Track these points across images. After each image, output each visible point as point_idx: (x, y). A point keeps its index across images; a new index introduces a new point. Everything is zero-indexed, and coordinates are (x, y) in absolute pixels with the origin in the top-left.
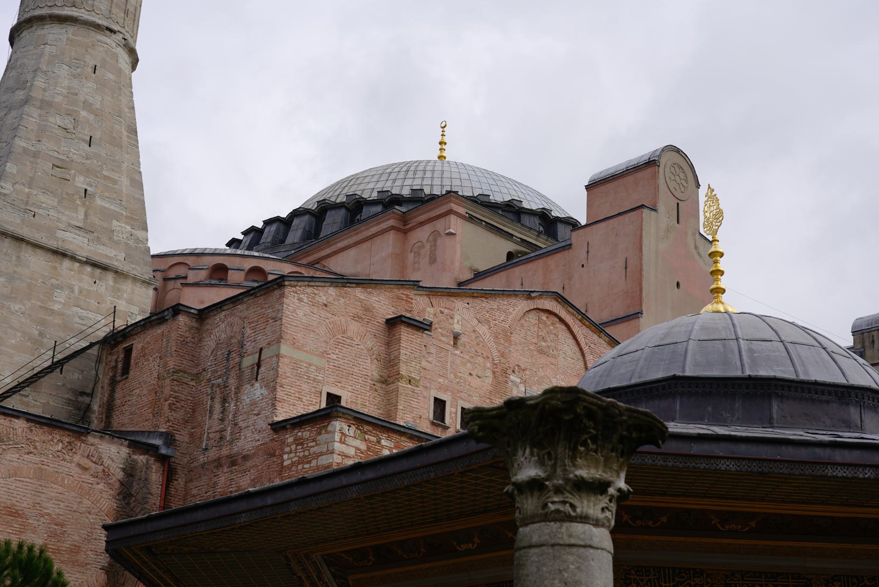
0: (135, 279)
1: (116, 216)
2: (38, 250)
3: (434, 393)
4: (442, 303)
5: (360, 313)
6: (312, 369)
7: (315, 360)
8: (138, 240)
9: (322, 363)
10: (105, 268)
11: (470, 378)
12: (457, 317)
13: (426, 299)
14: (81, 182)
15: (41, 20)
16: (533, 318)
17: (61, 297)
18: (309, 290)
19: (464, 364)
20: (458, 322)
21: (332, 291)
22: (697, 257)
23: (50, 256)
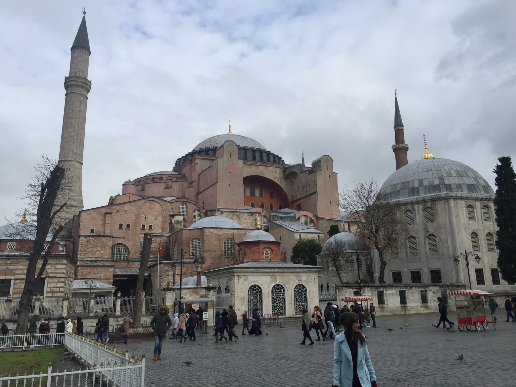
0: (79, 207)
1: (75, 196)
3: (119, 223)
4: (122, 206)
7: (88, 224)
8: (80, 199)
11: (129, 218)
12: (126, 207)
13: (117, 206)
16: (148, 202)
19: (128, 216)
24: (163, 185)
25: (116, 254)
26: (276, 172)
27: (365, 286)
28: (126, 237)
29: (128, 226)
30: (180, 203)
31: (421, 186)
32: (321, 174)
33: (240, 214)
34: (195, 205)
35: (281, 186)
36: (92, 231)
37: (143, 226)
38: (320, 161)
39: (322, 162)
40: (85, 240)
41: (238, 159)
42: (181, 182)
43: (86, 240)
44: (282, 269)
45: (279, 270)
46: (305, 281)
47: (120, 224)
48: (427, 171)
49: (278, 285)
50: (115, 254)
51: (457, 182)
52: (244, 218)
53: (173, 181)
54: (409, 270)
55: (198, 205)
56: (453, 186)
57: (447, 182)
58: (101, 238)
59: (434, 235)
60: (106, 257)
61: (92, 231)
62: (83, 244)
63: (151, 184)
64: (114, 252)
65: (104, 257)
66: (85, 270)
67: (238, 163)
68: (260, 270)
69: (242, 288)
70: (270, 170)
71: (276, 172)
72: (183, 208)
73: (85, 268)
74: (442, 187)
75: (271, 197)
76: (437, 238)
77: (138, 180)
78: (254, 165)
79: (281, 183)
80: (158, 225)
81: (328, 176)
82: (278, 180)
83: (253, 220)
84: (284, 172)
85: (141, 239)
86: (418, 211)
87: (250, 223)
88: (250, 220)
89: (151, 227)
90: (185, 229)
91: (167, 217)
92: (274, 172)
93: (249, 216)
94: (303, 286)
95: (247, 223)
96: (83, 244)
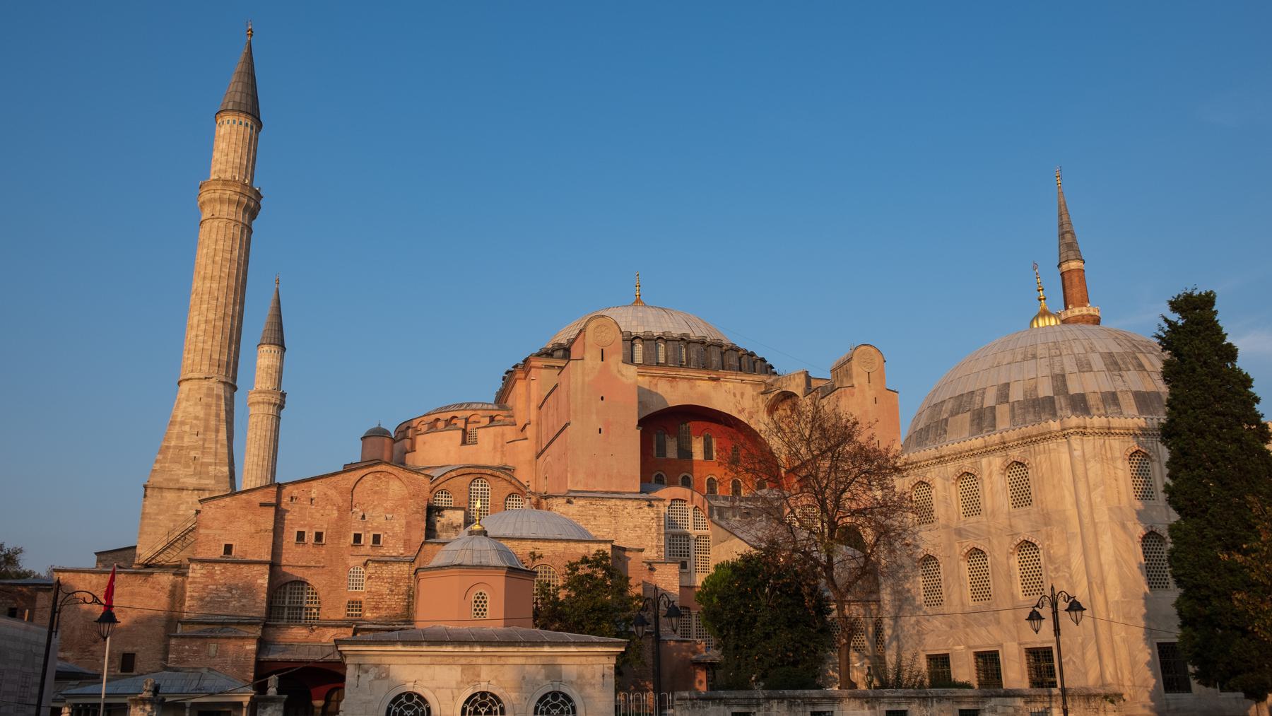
2: (170, 491)
5: (244, 505)
6: (217, 536)
7: (219, 532)
8: (222, 472)
9: (223, 531)
10: (203, 490)
12: (314, 490)
14: (193, 454)
15: (181, 381)
16: (370, 477)
17: (183, 507)
18: (215, 502)
19: (318, 511)
20: (314, 493)
21: (228, 499)
22: (620, 377)
23: (176, 491)
24: (458, 435)
25: (289, 608)
26: (742, 394)
27: (768, 699)
28: (313, 564)
29: (319, 536)
31: (1002, 403)
32: (853, 395)
36: (228, 549)
37: (357, 538)
38: (849, 360)
39: (854, 362)
40: (202, 571)
41: (623, 362)
42: (498, 428)
43: (204, 571)
44: (495, 646)
45: (485, 649)
46: (572, 682)
47: (299, 533)
48: (1024, 359)
49: (483, 694)
50: (286, 610)
51: (1107, 387)
52: (628, 513)
53: (481, 425)
54: (969, 647)
55: (517, 483)
56: (1092, 401)
57: (1074, 388)
58: (242, 566)
59: (1034, 545)
60: (254, 614)
61: (228, 549)
62: (195, 582)
64: (284, 602)
65: (247, 614)
66: (187, 647)
67: (624, 372)
68: (424, 649)
69: (369, 702)
71: (742, 394)
72: (479, 492)
73: (187, 640)
74: (1061, 402)
75: (734, 462)
76: (1041, 552)
77: (405, 425)
78: (683, 378)
80: (395, 535)
81: (870, 400)
83: (653, 519)
85: (352, 570)
86: (990, 475)
87: (643, 526)
88: (642, 518)
89: (376, 539)
90: (432, 543)
91: (418, 512)
93: (640, 508)
94: (565, 696)
95: (635, 526)
96: (195, 582)
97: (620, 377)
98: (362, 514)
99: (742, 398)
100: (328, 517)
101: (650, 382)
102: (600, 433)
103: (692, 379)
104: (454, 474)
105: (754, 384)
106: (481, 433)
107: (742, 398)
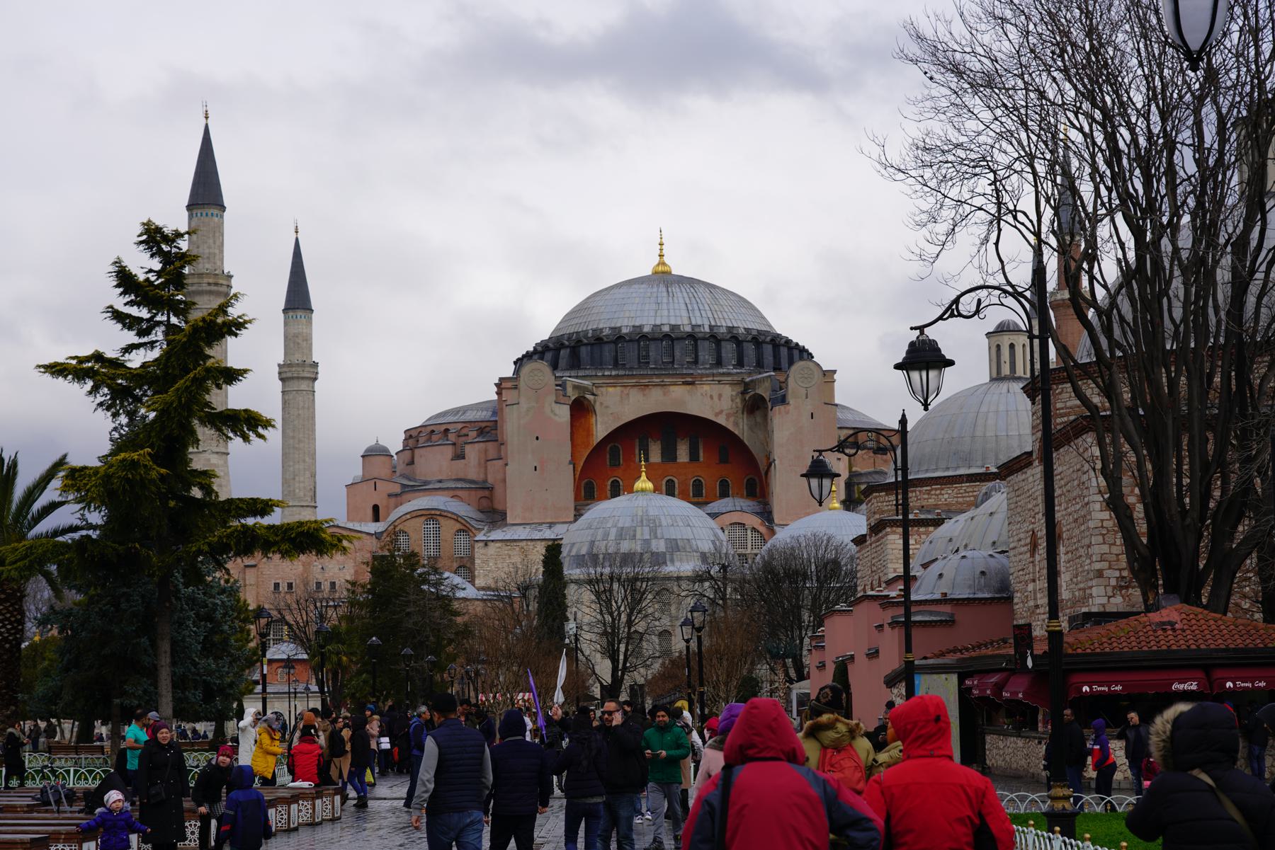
22: (552, 416)
24: (449, 451)
25: (274, 640)
26: (720, 396)
30: (423, 519)
32: (787, 413)
33: (527, 545)
34: (457, 520)
35: (736, 432)
42: (481, 444)
63: (424, 449)
67: (557, 411)
70: (702, 394)
71: (720, 396)
79: (736, 424)
82: (728, 416)
84: (743, 393)
92: (716, 398)
97: (552, 416)
98: (320, 566)
99: (720, 400)
100: (295, 571)
101: (622, 392)
102: (536, 470)
103: (665, 385)
104: (408, 516)
105: (732, 384)
106: (468, 448)
107: (720, 400)
